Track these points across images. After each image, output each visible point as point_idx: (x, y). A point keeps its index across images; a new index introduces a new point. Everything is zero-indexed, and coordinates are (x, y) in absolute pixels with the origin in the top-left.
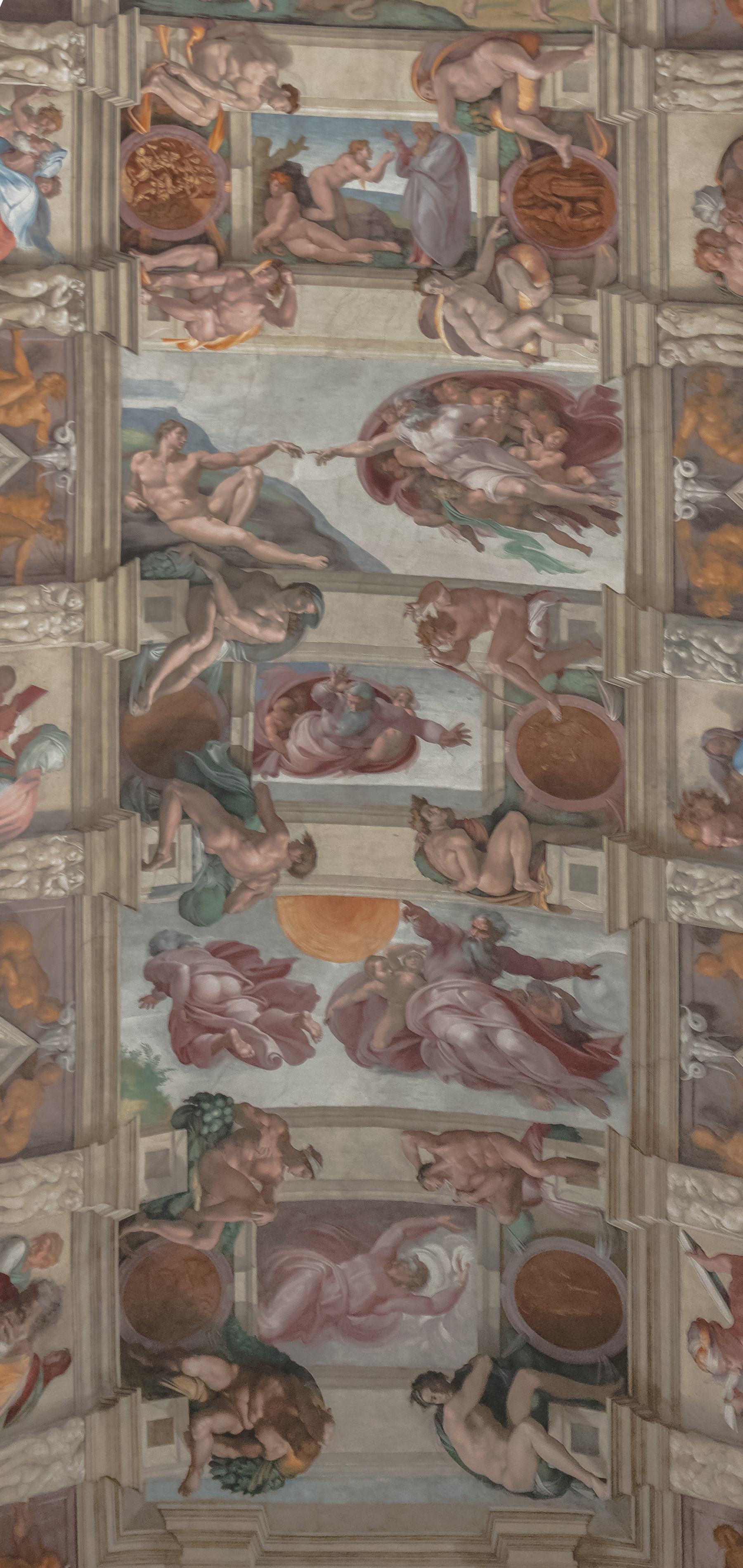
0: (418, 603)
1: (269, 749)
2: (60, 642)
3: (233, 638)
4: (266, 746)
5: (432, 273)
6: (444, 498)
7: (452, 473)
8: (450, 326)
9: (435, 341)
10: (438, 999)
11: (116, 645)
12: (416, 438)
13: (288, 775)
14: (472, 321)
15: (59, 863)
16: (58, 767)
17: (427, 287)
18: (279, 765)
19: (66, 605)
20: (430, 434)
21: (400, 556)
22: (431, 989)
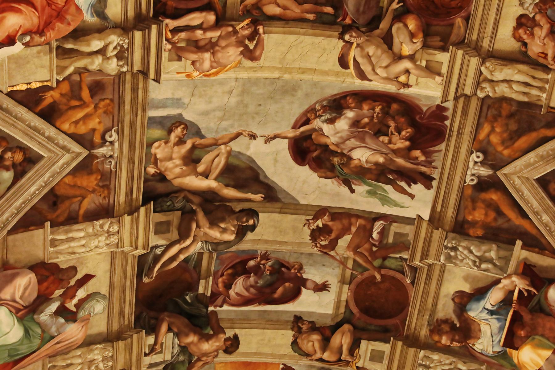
7: (344, 149)
8: (358, 63)
9: (347, 71)
11: (136, 248)
12: (327, 129)
13: (229, 306)
15: (100, 358)
16: (101, 312)
17: (347, 37)
18: (224, 302)
19: (108, 230)
20: (335, 126)
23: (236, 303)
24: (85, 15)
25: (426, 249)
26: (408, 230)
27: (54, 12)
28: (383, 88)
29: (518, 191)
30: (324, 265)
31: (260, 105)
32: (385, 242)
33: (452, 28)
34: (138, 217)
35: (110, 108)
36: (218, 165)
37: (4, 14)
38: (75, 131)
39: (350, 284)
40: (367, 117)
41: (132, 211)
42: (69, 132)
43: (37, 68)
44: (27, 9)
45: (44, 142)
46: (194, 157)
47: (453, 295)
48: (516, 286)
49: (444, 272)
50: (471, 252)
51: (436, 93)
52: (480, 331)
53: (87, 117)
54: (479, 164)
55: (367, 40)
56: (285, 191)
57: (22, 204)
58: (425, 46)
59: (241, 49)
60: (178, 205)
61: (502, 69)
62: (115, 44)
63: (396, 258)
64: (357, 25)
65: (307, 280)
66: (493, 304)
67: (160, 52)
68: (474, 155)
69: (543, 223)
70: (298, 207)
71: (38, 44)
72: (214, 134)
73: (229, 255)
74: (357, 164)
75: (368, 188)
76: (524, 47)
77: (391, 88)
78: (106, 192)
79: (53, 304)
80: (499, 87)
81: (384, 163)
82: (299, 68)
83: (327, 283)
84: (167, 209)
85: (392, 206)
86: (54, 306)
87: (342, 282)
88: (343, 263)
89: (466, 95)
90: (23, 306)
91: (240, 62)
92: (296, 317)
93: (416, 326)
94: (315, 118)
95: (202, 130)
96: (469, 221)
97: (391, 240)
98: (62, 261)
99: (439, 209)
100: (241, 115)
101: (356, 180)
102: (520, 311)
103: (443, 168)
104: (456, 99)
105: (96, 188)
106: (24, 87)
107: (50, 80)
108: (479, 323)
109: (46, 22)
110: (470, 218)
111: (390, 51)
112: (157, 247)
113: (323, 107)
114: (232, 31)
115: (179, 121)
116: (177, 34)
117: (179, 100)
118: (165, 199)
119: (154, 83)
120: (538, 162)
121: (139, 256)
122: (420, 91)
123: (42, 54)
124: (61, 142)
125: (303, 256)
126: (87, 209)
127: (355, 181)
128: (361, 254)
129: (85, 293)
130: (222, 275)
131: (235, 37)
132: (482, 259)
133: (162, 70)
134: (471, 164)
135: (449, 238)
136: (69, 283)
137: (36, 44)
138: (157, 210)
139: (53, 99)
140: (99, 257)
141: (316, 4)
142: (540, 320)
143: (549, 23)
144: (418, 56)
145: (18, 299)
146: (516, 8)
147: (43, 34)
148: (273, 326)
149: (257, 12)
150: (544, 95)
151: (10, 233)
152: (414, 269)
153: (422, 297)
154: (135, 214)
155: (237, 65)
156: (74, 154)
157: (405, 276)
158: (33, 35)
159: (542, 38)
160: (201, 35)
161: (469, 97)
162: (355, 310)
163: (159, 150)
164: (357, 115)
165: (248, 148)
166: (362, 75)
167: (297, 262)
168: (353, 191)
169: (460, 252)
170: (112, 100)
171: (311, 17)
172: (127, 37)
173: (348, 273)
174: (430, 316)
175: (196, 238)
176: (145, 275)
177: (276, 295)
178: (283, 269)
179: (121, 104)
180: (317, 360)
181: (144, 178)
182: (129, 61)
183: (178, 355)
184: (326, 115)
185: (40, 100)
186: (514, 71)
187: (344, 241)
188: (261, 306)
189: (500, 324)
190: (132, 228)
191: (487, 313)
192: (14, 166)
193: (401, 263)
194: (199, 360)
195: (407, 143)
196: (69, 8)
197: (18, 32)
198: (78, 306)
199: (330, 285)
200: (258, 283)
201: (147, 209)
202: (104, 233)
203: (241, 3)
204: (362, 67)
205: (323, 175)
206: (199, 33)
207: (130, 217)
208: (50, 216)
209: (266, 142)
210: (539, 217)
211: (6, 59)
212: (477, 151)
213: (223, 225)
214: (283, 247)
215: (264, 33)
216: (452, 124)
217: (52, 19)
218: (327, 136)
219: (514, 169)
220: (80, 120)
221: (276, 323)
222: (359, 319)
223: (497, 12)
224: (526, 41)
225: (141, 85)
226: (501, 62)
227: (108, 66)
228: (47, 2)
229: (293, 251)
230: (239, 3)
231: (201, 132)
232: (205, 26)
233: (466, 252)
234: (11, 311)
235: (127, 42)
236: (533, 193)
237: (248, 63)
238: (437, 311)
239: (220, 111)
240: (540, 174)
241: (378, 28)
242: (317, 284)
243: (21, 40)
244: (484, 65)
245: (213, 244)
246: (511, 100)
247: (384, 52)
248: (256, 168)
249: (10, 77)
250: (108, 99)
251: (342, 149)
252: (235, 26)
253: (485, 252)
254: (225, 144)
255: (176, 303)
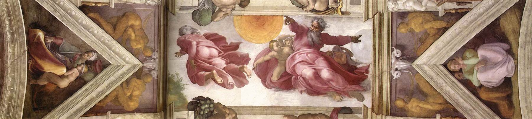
10: (298, 58)
22: (296, 54)
180: (311, 11)
183: (204, 3)
194: (220, 10)
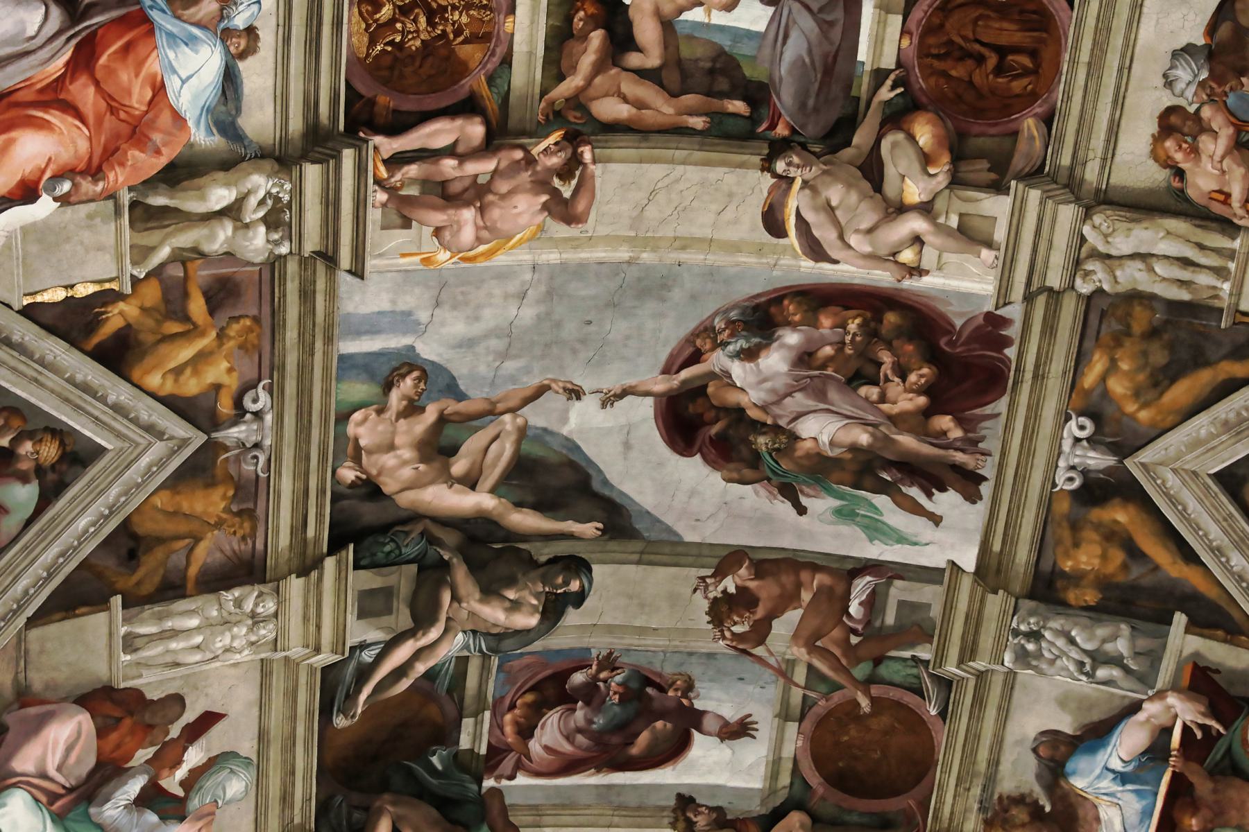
0: (713, 576)
1: (505, 751)
2: (246, 656)
3: (471, 627)
4: (504, 747)
5: (791, 148)
6: (764, 448)
7: (781, 417)
8: (807, 224)
9: (782, 241)
11: (318, 650)
12: (739, 371)
14: (835, 216)
17: (780, 166)
18: (518, 767)
19: (252, 611)
20: (758, 365)
21: (698, 520)
23: (544, 770)
24: (193, 131)
25: (970, 638)
26: (930, 595)
27: (124, 125)
28: (863, 278)
29: (1173, 501)
30: (741, 679)
31: (589, 323)
32: (878, 624)
33: (1016, 141)
34: (320, 579)
35: (252, 337)
36: (499, 457)
37: (13, 134)
38: (177, 391)
39: (801, 720)
40: (830, 344)
41: (307, 566)
42: (162, 393)
43: (87, 251)
44: (63, 121)
45: (107, 416)
46: (444, 441)
47: (1035, 739)
48: (1176, 716)
49: (1012, 688)
50: (1072, 641)
51: (985, 286)
52: (1098, 819)
53: (201, 358)
54: (1085, 443)
55: (825, 172)
56: (648, 513)
57: (58, 558)
58: (956, 181)
59: (544, 198)
60: (410, 551)
61: (1129, 229)
62: (261, 194)
63: (905, 660)
64: (802, 140)
65: (704, 713)
66: (1125, 758)
67: (361, 210)
68: (1072, 424)
69: (1233, 574)
70: (680, 549)
71: (90, 197)
72: (487, 390)
73: (526, 660)
74: (809, 449)
75: (836, 503)
76: (1177, 179)
77: (882, 277)
78: (247, 525)
79: (130, 782)
80: (1123, 270)
81: (870, 446)
82: (676, 238)
83: (749, 720)
84: (384, 561)
85: (891, 542)
86: (134, 787)
87: (784, 715)
88: (784, 672)
89: (1051, 290)
90: (64, 787)
91: (541, 228)
92: (680, 797)
93: (952, 813)
94: (713, 349)
95: (460, 382)
96: (1065, 572)
97: (890, 619)
98: (150, 683)
99: (997, 547)
100: (547, 346)
101: (809, 486)
102: (1187, 774)
103: (1003, 454)
104: (1029, 298)
105: (224, 516)
106: (59, 295)
107: (118, 277)
108: (1096, 802)
109: (105, 149)
110: (1068, 565)
111: (878, 195)
112: (363, 646)
113: (730, 323)
114: (522, 159)
115: (407, 363)
116: (400, 169)
117: (409, 314)
118: (382, 540)
119: (349, 278)
120: (1218, 436)
121: (323, 669)
122: (947, 282)
123: (98, 220)
124: (144, 416)
125: (694, 659)
126: (204, 564)
127: (808, 487)
128: (825, 653)
129: (202, 754)
130: (512, 707)
131: (529, 173)
132: (1099, 658)
133: (368, 249)
134: (1067, 445)
135: (1022, 612)
136: (167, 733)
137: (84, 198)
138: (363, 563)
139: (125, 320)
140: (233, 671)
141: (709, 93)
142: (1233, 794)
143: (1233, 124)
144: (940, 205)
145: (52, 772)
146: (1158, 93)
147: (101, 175)
148: (630, 820)
149: (578, 114)
150: (1226, 286)
151: (32, 622)
152: (946, 685)
153: (964, 746)
154: (313, 573)
155: (535, 234)
156: (174, 442)
157: (924, 699)
158: (78, 179)
159: (1217, 158)
160: (454, 168)
161: (1059, 293)
162: (814, 780)
163: (363, 429)
164: (809, 340)
165: (564, 420)
166: (816, 250)
167: (680, 674)
168: (802, 510)
169: (1049, 641)
170: (256, 320)
171: (698, 122)
172: (287, 178)
173: (797, 695)
174: (983, 791)
175: (452, 624)
176: (339, 710)
177: (635, 750)
178: (649, 690)
179: (277, 326)
181: (333, 493)
182: (293, 232)
184: (736, 342)
185: (95, 323)
186: (1157, 233)
187: (786, 625)
188: (601, 775)
189: (1144, 803)
190: (306, 606)
191: (1114, 779)
192: (40, 471)
193: (915, 671)
195: (922, 400)
196: (157, 117)
197: (43, 172)
198: (189, 784)
199: (757, 723)
200: (594, 723)
201: (339, 562)
202: (245, 617)
203: (542, 97)
204: (816, 233)
205: (735, 475)
206: (449, 164)
207: (302, 580)
208: (121, 583)
209: (604, 406)
210: (1223, 560)
211: (18, 231)
212: (1080, 414)
213: (511, 594)
214: (650, 641)
215: (594, 162)
216: (1020, 355)
217: (120, 142)
218: (742, 389)
219: (1163, 452)
220: (186, 364)
221: (637, 814)
222: (823, 798)
223: (1115, 101)
224: (1180, 165)
225: (321, 285)
226: (1128, 215)
227: (248, 243)
228: (108, 104)
229: (670, 649)
230: (537, 97)
231: (457, 386)
232: (461, 149)
233: (1061, 642)
234: (37, 800)
235: (289, 189)
236: (1208, 504)
237: (560, 230)
238: (999, 776)
239: (498, 337)
240: (1223, 462)
241: (848, 144)
242: (726, 724)
243: (50, 190)
244: (1089, 222)
245: (490, 637)
246: (1153, 297)
247: (863, 196)
248: (583, 464)
249: (28, 272)
250: (247, 316)
251: (775, 417)
252: (529, 148)
253: (1104, 641)
254: (512, 410)
255: (410, 773)
